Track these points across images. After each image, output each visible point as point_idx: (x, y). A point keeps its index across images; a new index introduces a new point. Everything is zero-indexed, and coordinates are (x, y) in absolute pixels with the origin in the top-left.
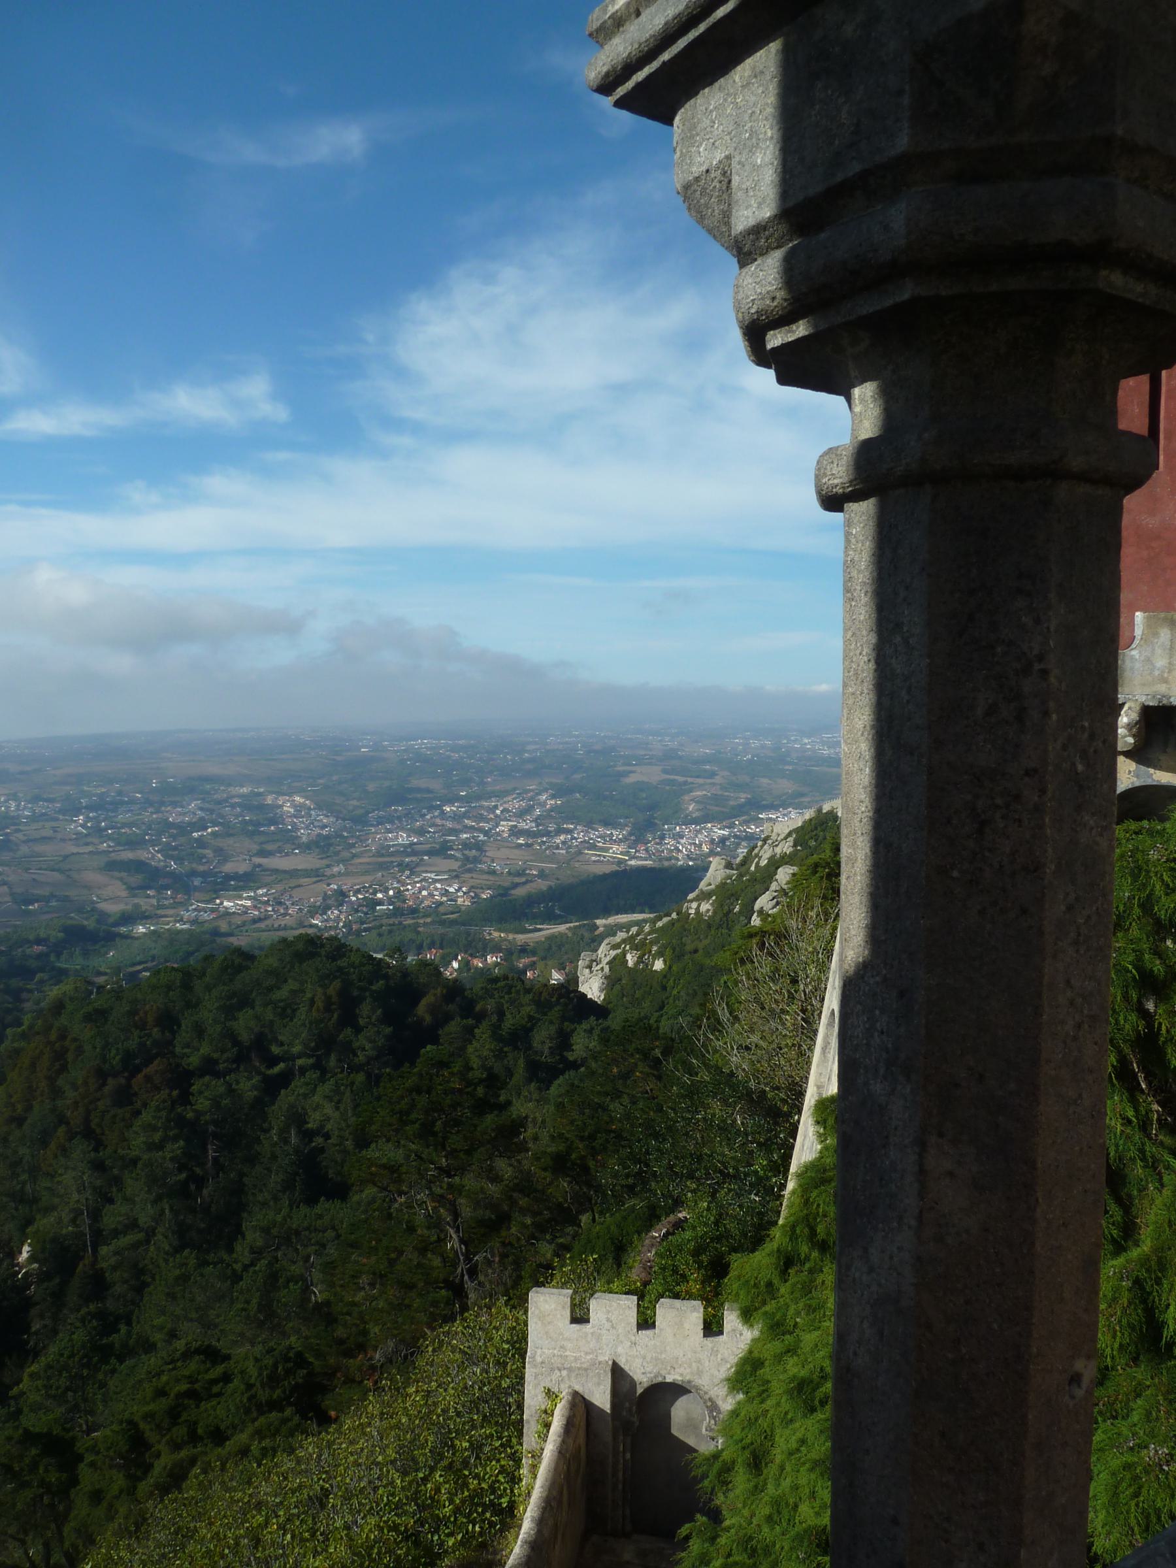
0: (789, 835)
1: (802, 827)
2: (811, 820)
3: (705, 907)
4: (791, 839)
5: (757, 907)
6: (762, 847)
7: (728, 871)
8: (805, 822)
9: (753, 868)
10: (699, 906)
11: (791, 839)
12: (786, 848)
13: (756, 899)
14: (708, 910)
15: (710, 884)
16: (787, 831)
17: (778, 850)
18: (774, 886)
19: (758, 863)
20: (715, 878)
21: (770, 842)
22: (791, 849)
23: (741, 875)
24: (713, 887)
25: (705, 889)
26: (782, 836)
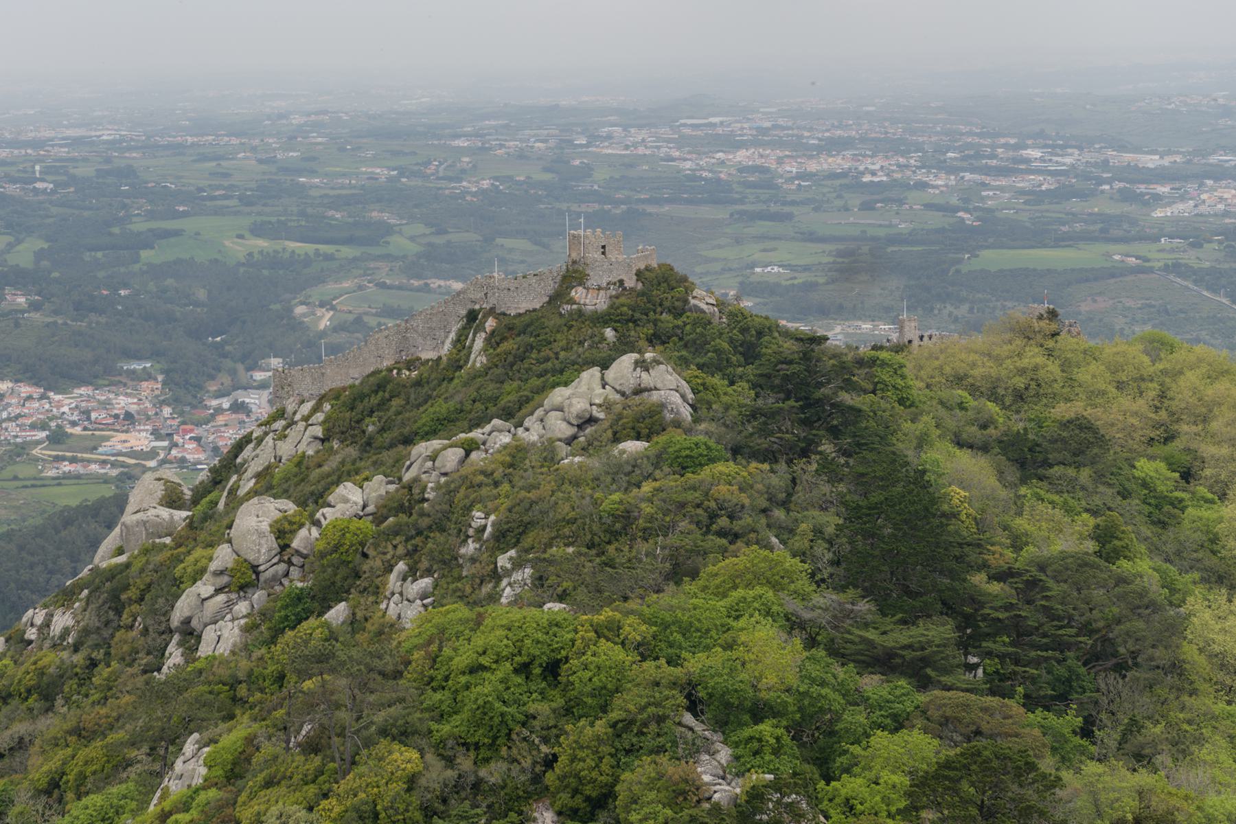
3: (62, 620)
4: (320, 417)
5: (176, 618)
6: (260, 441)
7: (165, 513)
10: (50, 616)
11: (320, 417)
12: (301, 441)
14: (66, 632)
15: (120, 551)
17: (286, 449)
18: (223, 556)
21: (279, 425)
23: (191, 525)
25: (104, 565)
26: (306, 408)
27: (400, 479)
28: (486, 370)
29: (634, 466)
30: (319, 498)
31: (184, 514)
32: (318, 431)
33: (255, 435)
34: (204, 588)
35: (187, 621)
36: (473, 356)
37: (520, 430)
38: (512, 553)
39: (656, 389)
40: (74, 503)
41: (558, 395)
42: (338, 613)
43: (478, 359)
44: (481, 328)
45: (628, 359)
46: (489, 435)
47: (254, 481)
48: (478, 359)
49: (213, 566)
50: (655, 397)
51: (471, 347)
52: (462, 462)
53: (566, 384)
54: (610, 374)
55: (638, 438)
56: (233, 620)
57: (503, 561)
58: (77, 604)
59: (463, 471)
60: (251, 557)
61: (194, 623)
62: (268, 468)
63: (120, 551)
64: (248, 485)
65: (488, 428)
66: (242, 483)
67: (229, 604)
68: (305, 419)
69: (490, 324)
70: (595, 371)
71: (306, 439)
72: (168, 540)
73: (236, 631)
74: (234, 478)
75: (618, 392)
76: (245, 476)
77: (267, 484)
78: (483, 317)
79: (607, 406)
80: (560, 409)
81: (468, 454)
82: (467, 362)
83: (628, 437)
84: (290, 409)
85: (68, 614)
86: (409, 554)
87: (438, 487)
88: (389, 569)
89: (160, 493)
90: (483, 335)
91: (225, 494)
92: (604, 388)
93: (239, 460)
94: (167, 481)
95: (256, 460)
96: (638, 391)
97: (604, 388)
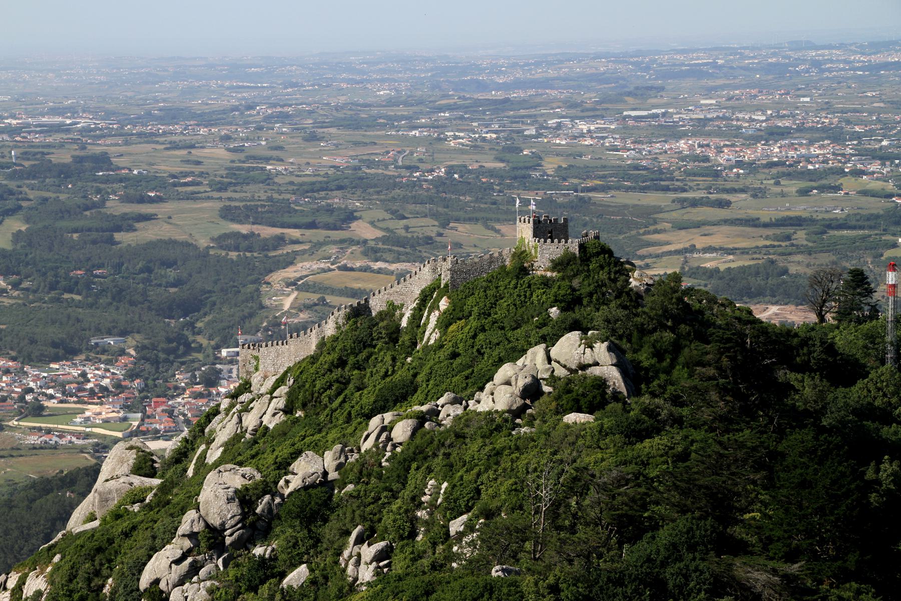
0: (280, 382)
1: (313, 359)
2: (335, 339)
4: (283, 390)
7: (137, 480)
8: (322, 345)
9: (190, 473)
11: (283, 390)
12: (266, 413)
13: (150, 557)
14: (39, 594)
15: (92, 518)
16: (282, 371)
17: (250, 421)
18: (189, 522)
19: (203, 456)
20: (104, 499)
22: (281, 417)
23: (164, 489)
24: (96, 524)
27: (359, 449)
28: (440, 346)
29: (577, 437)
30: (284, 466)
31: (156, 482)
32: (280, 403)
33: (223, 407)
34: (172, 551)
35: (157, 581)
36: (427, 334)
37: (471, 402)
38: (465, 517)
39: (597, 364)
40: (51, 473)
41: (506, 371)
42: (297, 576)
43: (431, 335)
44: (435, 306)
45: (575, 335)
46: (442, 406)
47: (221, 449)
48: (431, 335)
49: (180, 532)
50: (596, 371)
51: (426, 325)
52: (414, 432)
53: (514, 360)
54: (554, 352)
55: (579, 411)
56: (200, 581)
57: (456, 526)
58: (49, 569)
59: (418, 441)
60: (215, 521)
61: (162, 585)
62: (236, 438)
63: (92, 518)
64: (214, 455)
65: (441, 401)
66: (209, 451)
67: (194, 569)
68: (271, 392)
69: (444, 304)
70: (540, 350)
71: (270, 411)
72: (136, 507)
73: (203, 592)
74: (203, 447)
75: (565, 366)
76: (213, 446)
77: (234, 453)
78: (438, 295)
79: (553, 380)
80: (508, 383)
81: (421, 425)
82: (422, 339)
83: (572, 411)
84: (255, 379)
85: (41, 577)
86: (364, 519)
87: (394, 456)
88: (349, 533)
89: (131, 462)
90: (437, 313)
91: (194, 461)
92: (550, 363)
93: (207, 430)
94: (139, 449)
95: (223, 430)
96: (584, 367)
97: (550, 363)
